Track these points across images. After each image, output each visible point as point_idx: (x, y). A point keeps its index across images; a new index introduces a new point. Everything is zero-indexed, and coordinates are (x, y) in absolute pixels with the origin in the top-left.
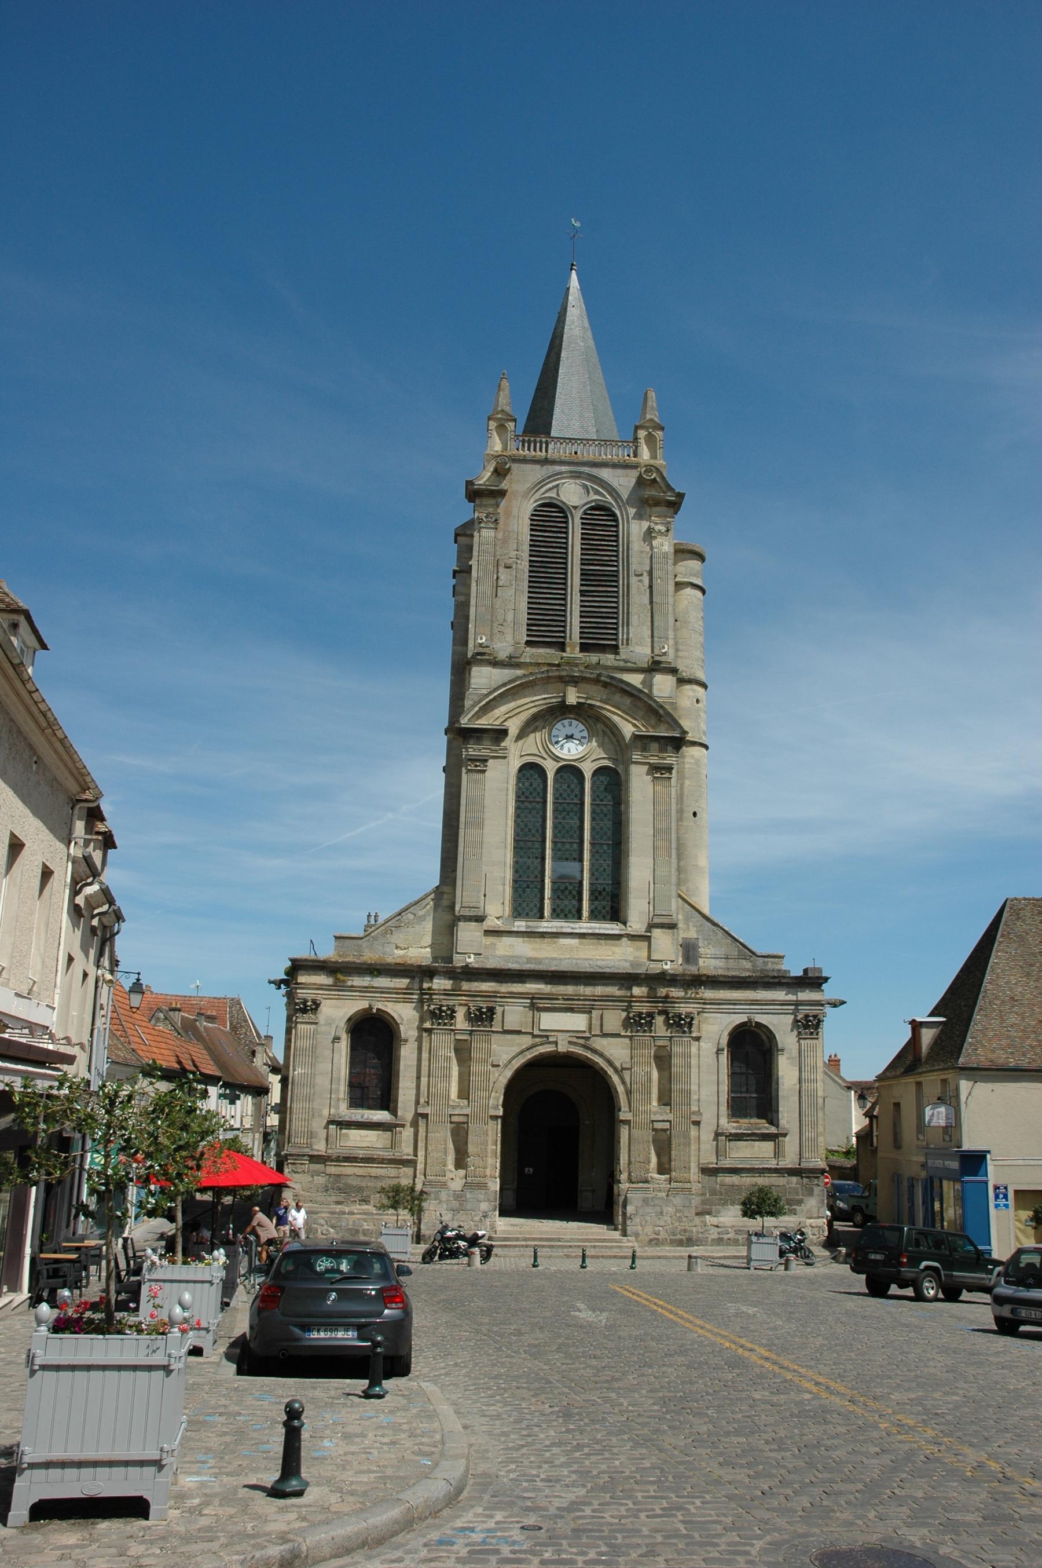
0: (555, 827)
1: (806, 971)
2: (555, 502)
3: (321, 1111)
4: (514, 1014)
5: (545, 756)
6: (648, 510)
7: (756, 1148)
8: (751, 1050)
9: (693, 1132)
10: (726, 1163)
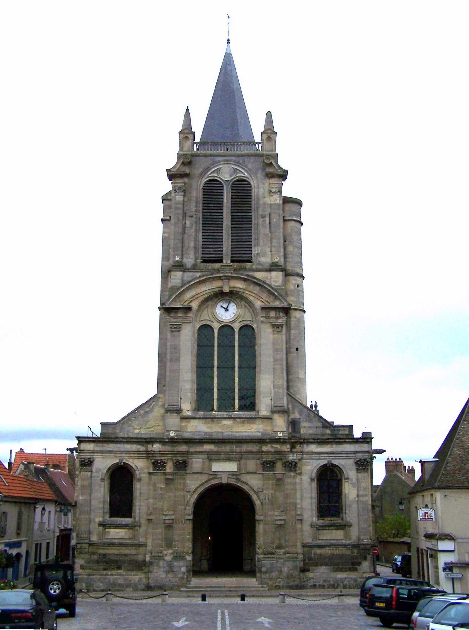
1: (363, 434)
2: (216, 178)
3: (94, 519)
4: (197, 463)
6: (268, 181)
8: (329, 481)
9: (299, 526)
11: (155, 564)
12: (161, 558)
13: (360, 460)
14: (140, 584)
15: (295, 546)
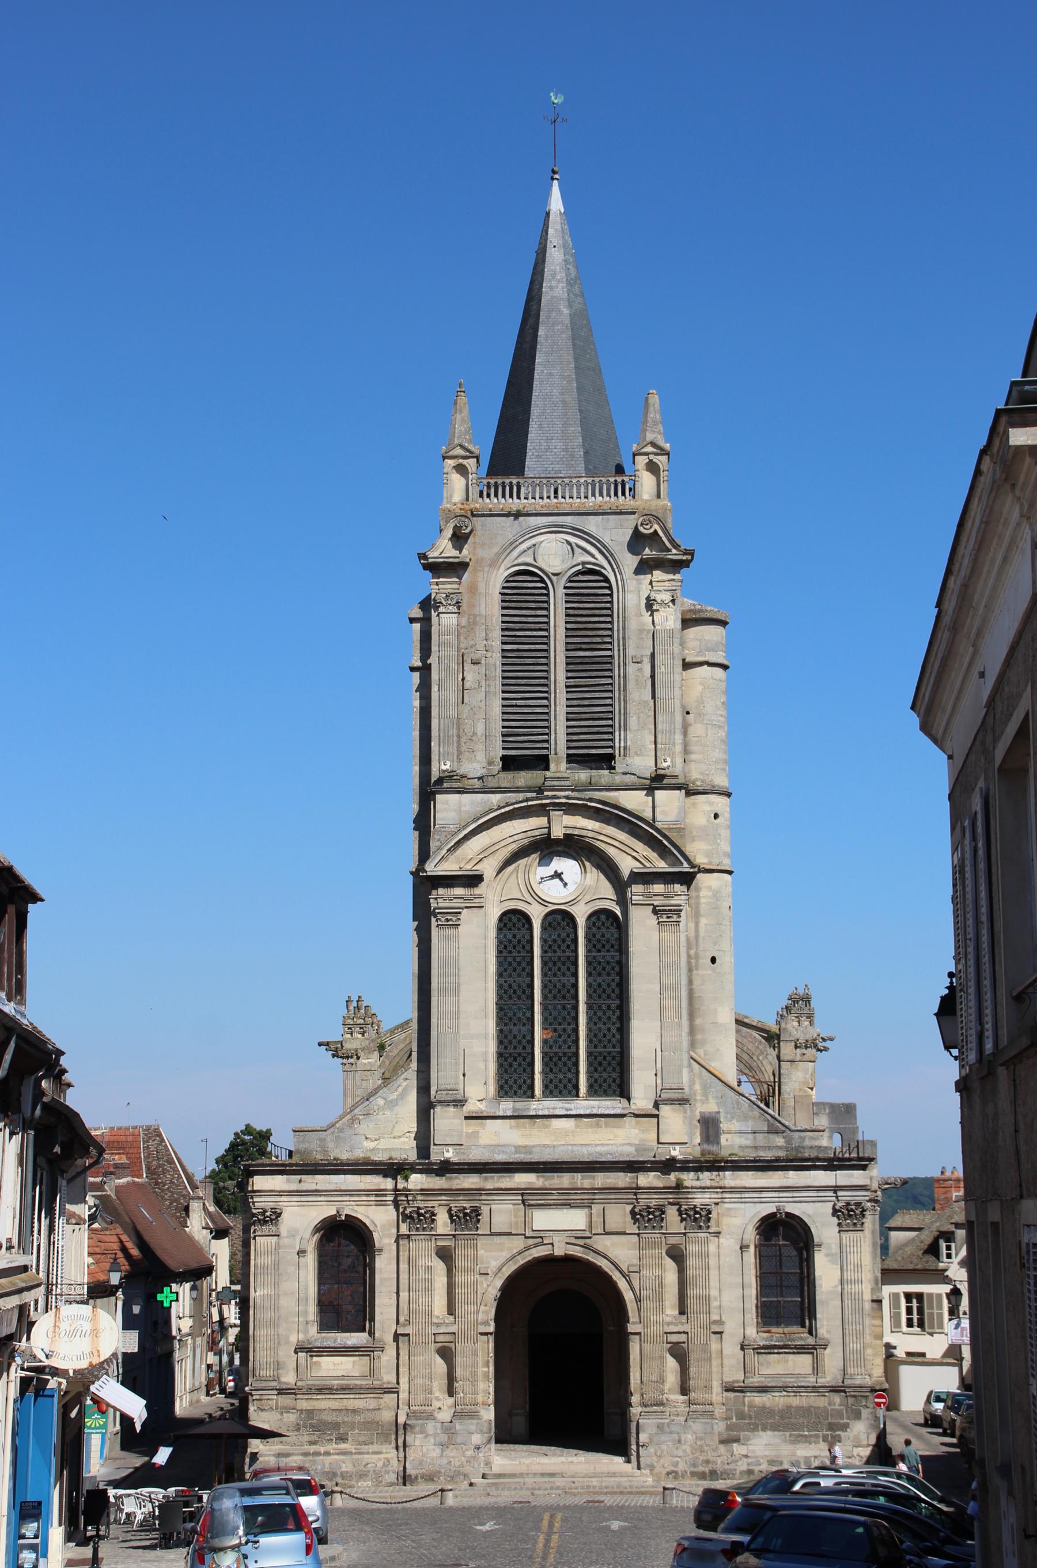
0: (544, 986)
3: (287, 1337)
4: (502, 1213)
5: (530, 899)
7: (790, 1363)
10: (755, 1381)
12: (430, 1416)
13: (848, 1204)
14: (387, 1472)
15: (709, 1388)
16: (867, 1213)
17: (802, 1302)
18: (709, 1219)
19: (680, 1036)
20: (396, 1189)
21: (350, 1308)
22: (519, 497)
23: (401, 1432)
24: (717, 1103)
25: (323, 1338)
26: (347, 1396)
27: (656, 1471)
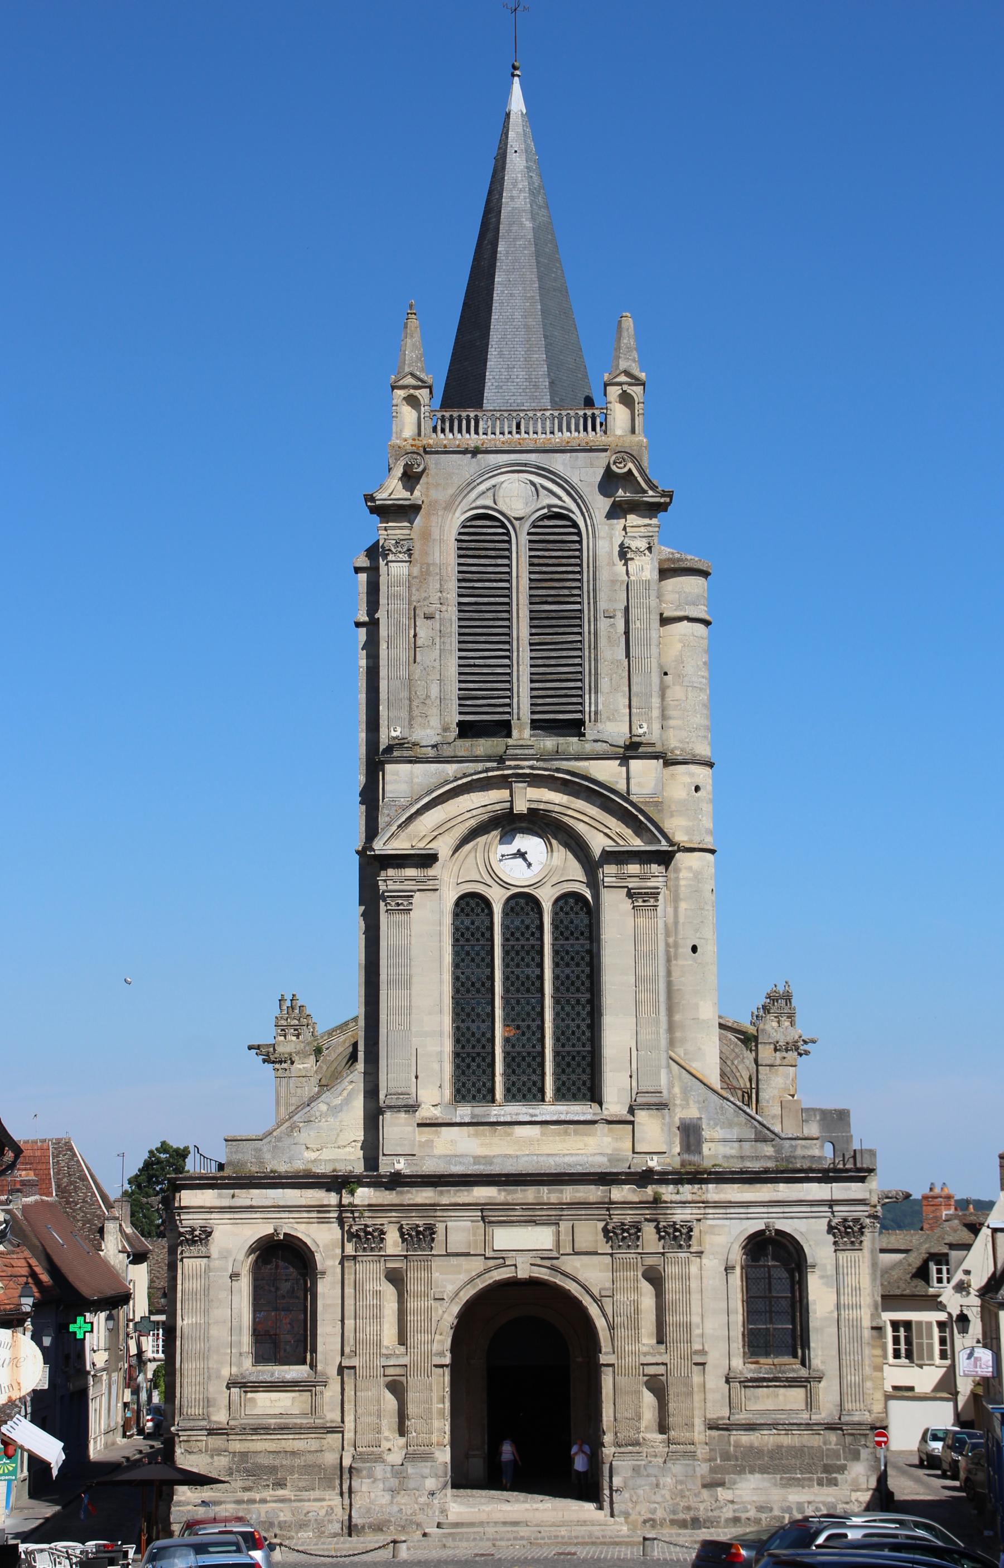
0: (506, 978)
3: (219, 1371)
4: (459, 1231)
5: (490, 881)
7: (781, 1398)
10: (741, 1417)
11: (364, 1472)
12: (379, 1459)
13: (845, 1220)
14: (330, 1521)
15: (690, 1426)
16: (865, 1230)
17: (794, 1330)
18: (690, 1237)
19: (658, 1033)
20: (340, 1205)
21: (289, 1337)
22: (477, 433)
23: (346, 1476)
24: (699, 1109)
25: (259, 1371)
26: (285, 1437)
27: (633, 1517)
